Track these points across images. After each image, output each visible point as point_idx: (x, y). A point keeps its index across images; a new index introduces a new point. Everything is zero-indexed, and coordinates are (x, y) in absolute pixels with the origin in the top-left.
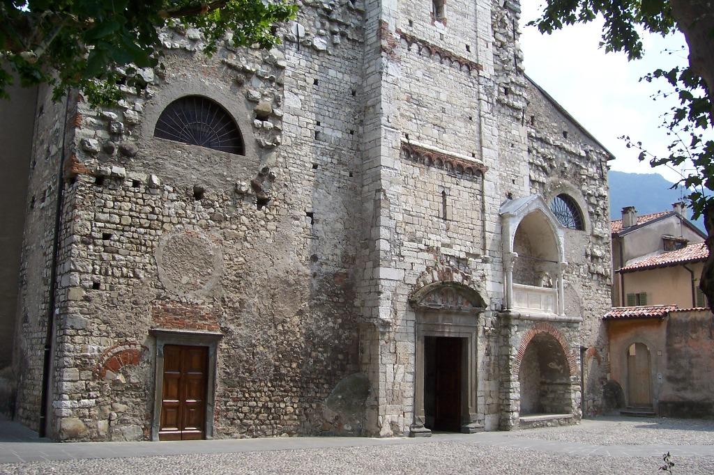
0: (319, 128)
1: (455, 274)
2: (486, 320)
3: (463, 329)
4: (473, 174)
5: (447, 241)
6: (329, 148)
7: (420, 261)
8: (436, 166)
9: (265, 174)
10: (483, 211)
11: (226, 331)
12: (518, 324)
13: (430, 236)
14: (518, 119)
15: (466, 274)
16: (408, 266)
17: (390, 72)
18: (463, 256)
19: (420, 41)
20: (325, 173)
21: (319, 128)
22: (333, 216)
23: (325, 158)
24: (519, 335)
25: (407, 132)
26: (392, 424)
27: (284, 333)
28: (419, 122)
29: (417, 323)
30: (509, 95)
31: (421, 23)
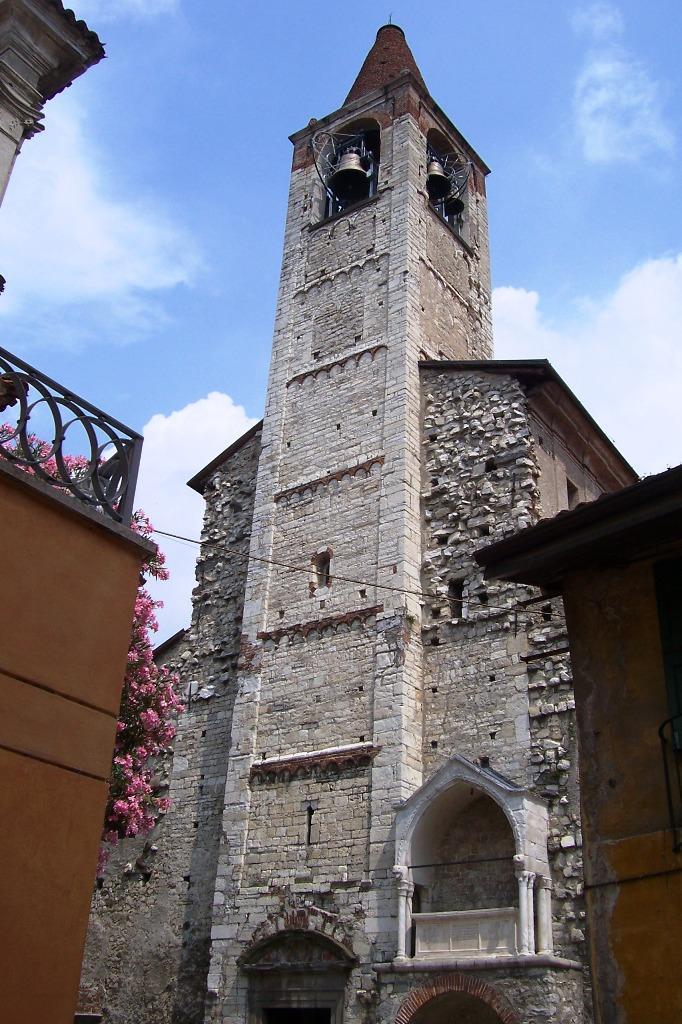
0: (203, 782)
1: (311, 917)
5: (306, 873)
7: (260, 909)
11: (105, 1011)
12: (393, 980)
13: (279, 873)
14: (507, 630)
16: (242, 919)
17: (245, 690)
18: (325, 888)
21: (203, 782)
24: (397, 999)
27: (154, 1011)
29: (250, 992)
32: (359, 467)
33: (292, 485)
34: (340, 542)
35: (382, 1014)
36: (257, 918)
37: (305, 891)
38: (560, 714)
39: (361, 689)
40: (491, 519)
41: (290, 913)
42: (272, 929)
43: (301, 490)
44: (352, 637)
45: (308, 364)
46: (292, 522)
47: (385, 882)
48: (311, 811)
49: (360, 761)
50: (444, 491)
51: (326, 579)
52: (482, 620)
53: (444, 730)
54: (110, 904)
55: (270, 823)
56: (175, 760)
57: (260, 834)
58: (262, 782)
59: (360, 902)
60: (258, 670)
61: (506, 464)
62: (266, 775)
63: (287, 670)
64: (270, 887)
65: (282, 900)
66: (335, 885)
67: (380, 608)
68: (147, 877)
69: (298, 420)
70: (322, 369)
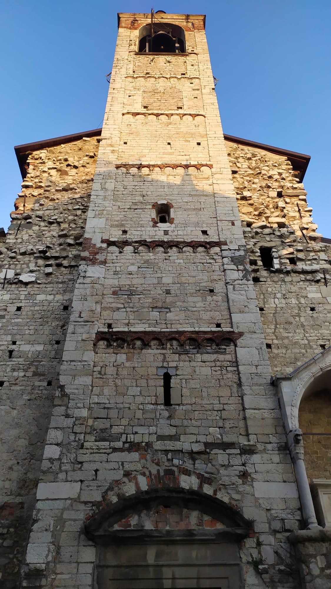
0: (13, 347)
3: (207, 571)
4: (217, 345)
6: (24, 363)
8: (153, 347)
10: (240, 385)
13: (135, 429)
15: (206, 475)
18: (196, 448)
19: (136, 242)
20: (12, 388)
21: (13, 347)
22: (14, 432)
23: (15, 374)
25: (110, 322)
28: (128, 309)
30: (298, 263)
31: (139, 229)
36: (108, 476)
37: (172, 448)
41: (154, 472)
42: (130, 489)
47: (269, 447)
53: (277, 337)
55: (119, 382)
58: (109, 346)
59: (244, 465)
64: (124, 443)
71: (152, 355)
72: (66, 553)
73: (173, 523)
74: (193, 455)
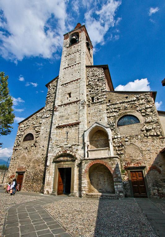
2: (77, 162)
5: (67, 143)
9: (36, 142)
11: (26, 170)
14: (102, 104)
18: (71, 146)
24: (86, 165)
26: (47, 191)
32: (76, 80)
33: (64, 83)
34: (72, 91)
35: (83, 168)
36: (57, 152)
38: (113, 116)
39: (77, 113)
40: (98, 88)
43: (65, 84)
44: (75, 104)
45: (67, 66)
46: (64, 88)
48: (67, 133)
49: (77, 124)
50: (90, 84)
51: (70, 97)
52: (98, 102)
54: (28, 151)
56: (42, 127)
57: (57, 137)
58: (58, 128)
60: (58, 111)
61: (100, 80)
62: (59, 127)
63: (63, 111)
65: (62, 148)
66: (72, 145)
67: (80, 100)
68: (36, 147)
69: (65, 74)
70: (69, 67)
71: (65, 129)
72: (51, 164)
73: (65, 158)
74: (70, 147)
